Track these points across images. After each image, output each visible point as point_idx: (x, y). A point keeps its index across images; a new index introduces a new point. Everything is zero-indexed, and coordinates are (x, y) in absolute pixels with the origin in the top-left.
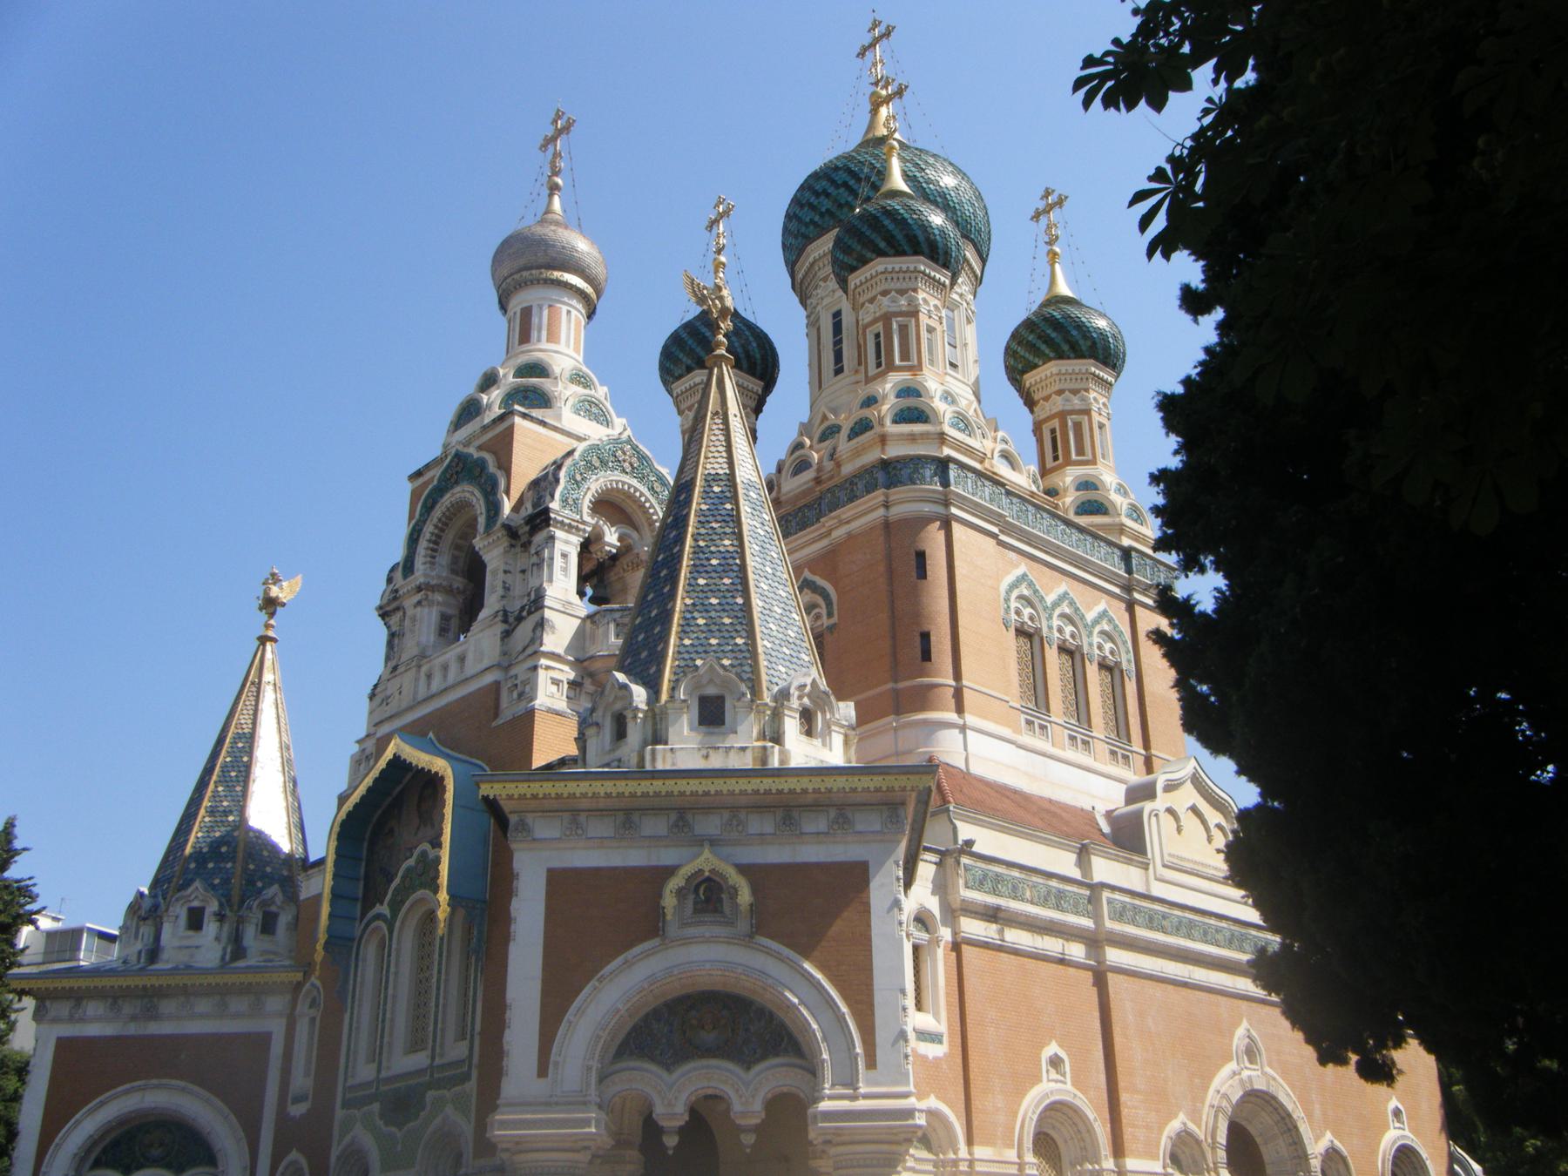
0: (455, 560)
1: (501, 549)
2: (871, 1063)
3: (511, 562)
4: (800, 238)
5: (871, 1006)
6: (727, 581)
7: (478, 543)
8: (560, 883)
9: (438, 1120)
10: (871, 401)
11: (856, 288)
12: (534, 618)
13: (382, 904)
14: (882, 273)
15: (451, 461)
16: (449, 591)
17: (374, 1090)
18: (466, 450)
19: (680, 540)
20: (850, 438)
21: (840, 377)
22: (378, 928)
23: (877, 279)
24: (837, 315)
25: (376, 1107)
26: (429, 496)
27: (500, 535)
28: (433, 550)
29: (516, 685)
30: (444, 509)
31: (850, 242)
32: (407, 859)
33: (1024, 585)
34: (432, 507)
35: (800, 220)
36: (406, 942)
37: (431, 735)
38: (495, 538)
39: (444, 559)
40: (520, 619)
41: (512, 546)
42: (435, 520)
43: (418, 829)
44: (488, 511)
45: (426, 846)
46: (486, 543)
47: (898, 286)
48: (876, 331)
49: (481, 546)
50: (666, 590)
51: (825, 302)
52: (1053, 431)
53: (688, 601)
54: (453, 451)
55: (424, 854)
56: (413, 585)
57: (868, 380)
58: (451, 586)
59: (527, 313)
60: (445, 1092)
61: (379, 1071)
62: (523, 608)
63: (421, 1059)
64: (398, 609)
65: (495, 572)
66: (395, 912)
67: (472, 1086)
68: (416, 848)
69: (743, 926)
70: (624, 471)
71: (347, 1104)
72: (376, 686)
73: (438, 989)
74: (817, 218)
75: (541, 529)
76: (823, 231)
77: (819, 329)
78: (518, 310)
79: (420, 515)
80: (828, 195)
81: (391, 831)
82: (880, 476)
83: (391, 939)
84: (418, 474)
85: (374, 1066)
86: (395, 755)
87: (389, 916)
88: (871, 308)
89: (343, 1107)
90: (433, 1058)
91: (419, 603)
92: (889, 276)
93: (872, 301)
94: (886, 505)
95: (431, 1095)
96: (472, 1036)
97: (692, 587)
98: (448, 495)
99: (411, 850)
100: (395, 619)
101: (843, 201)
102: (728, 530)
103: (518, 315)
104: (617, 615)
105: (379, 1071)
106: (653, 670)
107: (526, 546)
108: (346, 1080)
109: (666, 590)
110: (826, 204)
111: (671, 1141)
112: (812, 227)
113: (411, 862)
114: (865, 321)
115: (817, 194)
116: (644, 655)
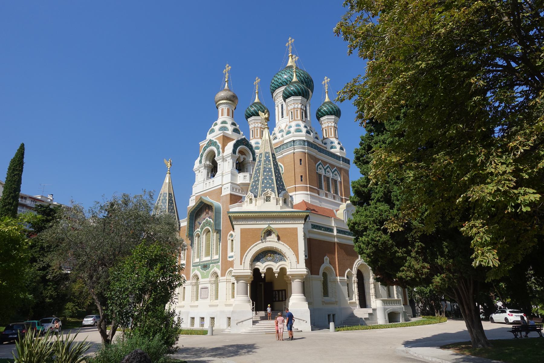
2: (298, 263)
5: (298, 253)
6: (270, 173)
7: (216, 159)
8: (243, 231)
9: (213, 270)
10: (290, 127)
19: (260, 165)
20: (286, 135)
21: (283, 118)
22: (198, 233)
24: (282, 105)
25: (200, 267)
26: (204, 148)
33: (321, 165)
34: (205, 150)
35: (274, 84)
36: (204, 237)
37: (208, 197)
44: (218, 153)
45: (208, 218)
50: (258, 175)
51: (280, 102)
52: (326, 130)
53: (263, 177)
55: (207, 219)
57: (290, 122)
59: (222, 110)
61: (200, 260)
63: (208, 258)
65: (220, 165)
66: (201, 231)
67: (220, 264)
69: (276, 239)
70: (244, 145)
71: (193, 266)
73: (212, 245)
76: (279, 87)
77: (278, 108)
78: (221, 108)
80: (281, 79)
82: (293, 143)
85: (199, 259)
90: (211, 258)
94: (294, 149)
95: (211, 265)
96: (219, 255)
97: (264, 174)
99: (205, 219)
102: (270, 163)
105: (200, 260)
106: (257, 190)
109: (258, 175)
110: (280, 81)
111: (263, 275)
113: (205, 221)
115: (278, 79)
116: (255, 187)
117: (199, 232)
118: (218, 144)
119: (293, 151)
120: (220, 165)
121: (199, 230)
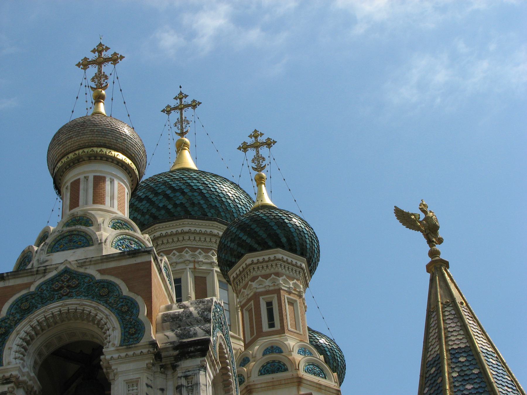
0: (35, 363)
1: (143, 364)
3: (152, 378)
4: (147, 217)
11: (253, 263)
14: (279, 260)
15: (60, 275)
18: (81, 270)
20: (261, 373)
23: (274, 263)
27: (145, 351)
28: (24, 348)
30: (48, 314)
31: (257, 230)
38: (138, 352)
39: (29, 361)
42: (34, 323)
46: (123, 355)
47: (263, 272)
48: (269, 300)
49: (116, 356)
54: (62, 267)
58: (33, 388)
74: (170, 207)
75: (191, 357)
79: (9, 313)
80: (183, 193)
88: (267, 282)
92: (256, 266)
93: (266, 277)
98: (60, 303)
101: (196, 201)
103: (91, 179)
107: (174, 367)
112: (163, 212)
118: (125, 291)
120: (131, 384)
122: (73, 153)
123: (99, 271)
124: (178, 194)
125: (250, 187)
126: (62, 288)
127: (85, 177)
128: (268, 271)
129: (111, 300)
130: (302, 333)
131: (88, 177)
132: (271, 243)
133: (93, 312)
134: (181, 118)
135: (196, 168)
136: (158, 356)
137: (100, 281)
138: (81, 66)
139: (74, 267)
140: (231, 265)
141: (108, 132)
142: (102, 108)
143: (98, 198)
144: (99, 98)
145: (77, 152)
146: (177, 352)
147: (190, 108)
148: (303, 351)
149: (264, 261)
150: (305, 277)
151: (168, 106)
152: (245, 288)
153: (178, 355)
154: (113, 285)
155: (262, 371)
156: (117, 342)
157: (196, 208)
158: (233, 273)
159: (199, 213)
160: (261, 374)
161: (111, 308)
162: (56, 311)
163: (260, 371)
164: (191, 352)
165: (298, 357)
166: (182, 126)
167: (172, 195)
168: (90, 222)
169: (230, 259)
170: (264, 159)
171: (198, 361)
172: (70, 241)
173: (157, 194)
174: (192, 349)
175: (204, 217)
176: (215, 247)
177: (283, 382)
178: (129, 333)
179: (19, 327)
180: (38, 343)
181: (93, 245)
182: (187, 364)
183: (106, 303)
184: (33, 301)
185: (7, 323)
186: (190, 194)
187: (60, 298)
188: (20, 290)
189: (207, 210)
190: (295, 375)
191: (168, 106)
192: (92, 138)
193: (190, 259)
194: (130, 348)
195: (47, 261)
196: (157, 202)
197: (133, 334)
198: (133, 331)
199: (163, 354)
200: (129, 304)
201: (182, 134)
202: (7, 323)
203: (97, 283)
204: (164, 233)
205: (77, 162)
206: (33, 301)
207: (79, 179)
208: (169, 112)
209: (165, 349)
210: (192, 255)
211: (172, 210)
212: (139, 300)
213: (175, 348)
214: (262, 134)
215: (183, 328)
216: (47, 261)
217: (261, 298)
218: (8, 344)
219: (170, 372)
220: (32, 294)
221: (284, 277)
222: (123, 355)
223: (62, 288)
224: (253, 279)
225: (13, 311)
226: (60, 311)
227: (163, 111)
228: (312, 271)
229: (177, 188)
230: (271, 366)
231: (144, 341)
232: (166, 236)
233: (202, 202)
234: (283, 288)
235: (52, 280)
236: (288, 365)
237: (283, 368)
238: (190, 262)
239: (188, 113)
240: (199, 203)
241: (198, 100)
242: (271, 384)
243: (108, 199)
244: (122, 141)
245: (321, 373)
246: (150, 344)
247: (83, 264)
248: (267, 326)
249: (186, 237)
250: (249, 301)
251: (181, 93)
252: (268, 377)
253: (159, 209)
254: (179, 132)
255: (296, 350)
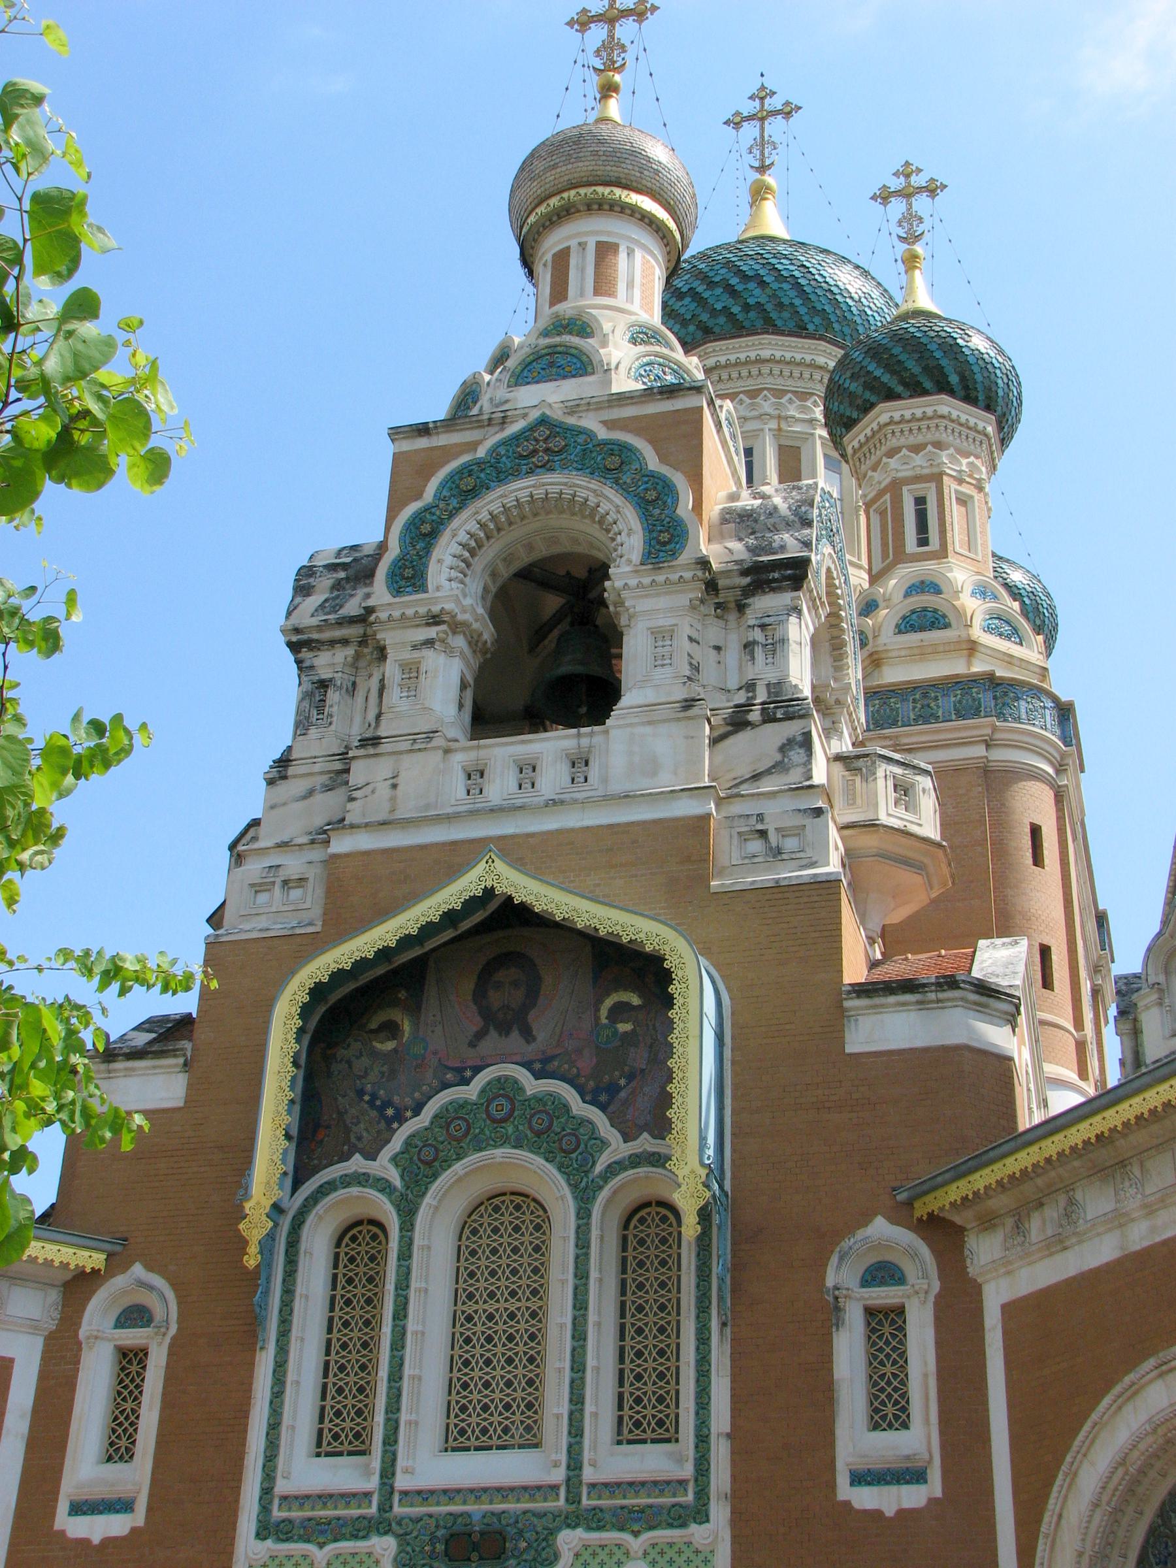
0: (486, 589)
1: (683, 600)
4: (692, 328)
11: (891, 422)
12: (792, 729)
13: (371, 1156)
14: (943, 417)
15: (532, 428)
16: (474, 642)
17: (374, 1509)
18: (571, 421)
23: (932, 423)
26: (465, 471)
27: (688, 575)
29: (763, 834)
30: (510, 501)
31: (903, 357)
32: (446, 1086)
38: (674, 577)
39: (475, 586)
40: (738, 722)
41: (702, 601)
42: (484, 516)
43: (480, 1035)
46: (646, 581)
47: (912, 440)
48: (920, 494)
49: (633, 582)
54: (534, 415)
56: (422, 610)
58: (481, 635)
60: (626, 1537)
62: (743, 709)
64: (345, 642)
68: (477, 1070)
72: (283, 763)
74: (736, 309)
75: (773, 590)
79: (438, 496)
80: (762, 284)
81: (391, 1029)
83: (407, 1226)
84: (423, 430)
85: (376, 1461)
86: (485, 889)
87: (397, 1182)
88: (919, 460)
89: (261, 1535)
91: (429, 643)
92: (897, 429)
93: (917, 449)
96: (702, 1439)
100: (328, 663)
101: (786, 301)
104: (898, 770)
107: (741, 608)
108: (269, 1476)
112: (722, 320)
113: (471, 1092)
114: (900, 475)
117: (384, 1186)
118: (653, 463)
119: (979, 751)
120: (661, 635)
121: (384, 1166)
122: (558, 197)
123: (604, 423)
124: (752, 285)
125: (889, 273)
126: (534, 452)
127: (580, 244)
128: (920, 439)
129: (626, 478)
130: (980, 558)
131: (586, 243)
132: (928, 385)
133: (593, 501)
134: (762, 136)
135: (788, 237)
136: (711, 586)
137: (605, 443)
138: (576, 26)
139: (557, 414)
140: (849, 424)
141: (625, 156)
142: (613, 108)
143: (603, 284)
144: (608, 90)
145: (565, 195)
146: (748, 580)
147: (779, 117)
148: (982, 591)
149: (914, 419)
150: (992, 453)
151: (737, 114)
152: (874, 469)
153: (749, 585)
154: (630, 450)
155: (902, 627)
156: (636, 557)
157: (786, 315)
158: (853, 440)
159: (791, 324)
160: (900, 632)
161: (625, 494)
162: (523, 495)
163: (897, 626)
164: (775, 580)
165: (971, 604)
166: (762, 154)
167: (739, 288)
168: (589, 330)
169: (848, 414)
170: (921, 220)
171: (785, 598)
172: (551, 364)
173: (711, 285)
174: (776, 575)
175: (800, 330)
176: (821, 390)
177: (941, 649)
178: (659, 542)
179: (456, 523)
180: (490, 552)
181: (593, 373)
182: (765, 603)
183: (616, 482)
184: (482, 475)
185: (434, 514)
186: (775, 286)
187: (531, 472)
188: (456, 456)
189: (806, 318)
190: (964, 635)
191: (737, 114)
192: (596, 168)
193: (771, 411)
194: (660, 568)
195: (507, 401)
196: (711, 301)
197: (664, 544)
198: (665, 537)
199: (722, 583)
200: (659, 487)
201: (762, 169)
202: (434, 514)
203: (599, 445)
204: (723, 360)
205: (566, 213)
206: (482, 475)
207: (568, 248)
208: (737, 125)
209: (726, 573)
210: (774, 404)
211: (740, 317)
212: (679, 480)
213: (745, 573)
214: (919, 170)
215: (759, 535)
216: (507, 401)
217: (905, 489)
218: (436, 554)
219: (732, 616)
220: (479, 463)
221: (951, 451)
222: (646, 581)
223: (534, 452)
224: (891, 453)
225: (445, 493)
226: (531, 496)
227: (727, 123)
228: (1004, 442)
229: (750, 273)
230: (918, 617)
231: (685, 557)
232: (726, 366)
233: (797, 302)
234: (948, 471)
235: (516, 438)
236: (952, 618)
237: (942, 621)
238: (772, 417)
239: (775, 127)
240: (792, 304)
241: (796, 101)
242: (916, 651)
243: (621, 287)
244: (652, 175)
245: (1015, 634)
246: (698, 563)
247: (574, 408)
248: (915, 542)
249: (765, 370)
250: (881, 494)
251: (763, 88)
252: (914, 638)
253: (714, 313)
254: (757, 164)
255: (968, 590)
